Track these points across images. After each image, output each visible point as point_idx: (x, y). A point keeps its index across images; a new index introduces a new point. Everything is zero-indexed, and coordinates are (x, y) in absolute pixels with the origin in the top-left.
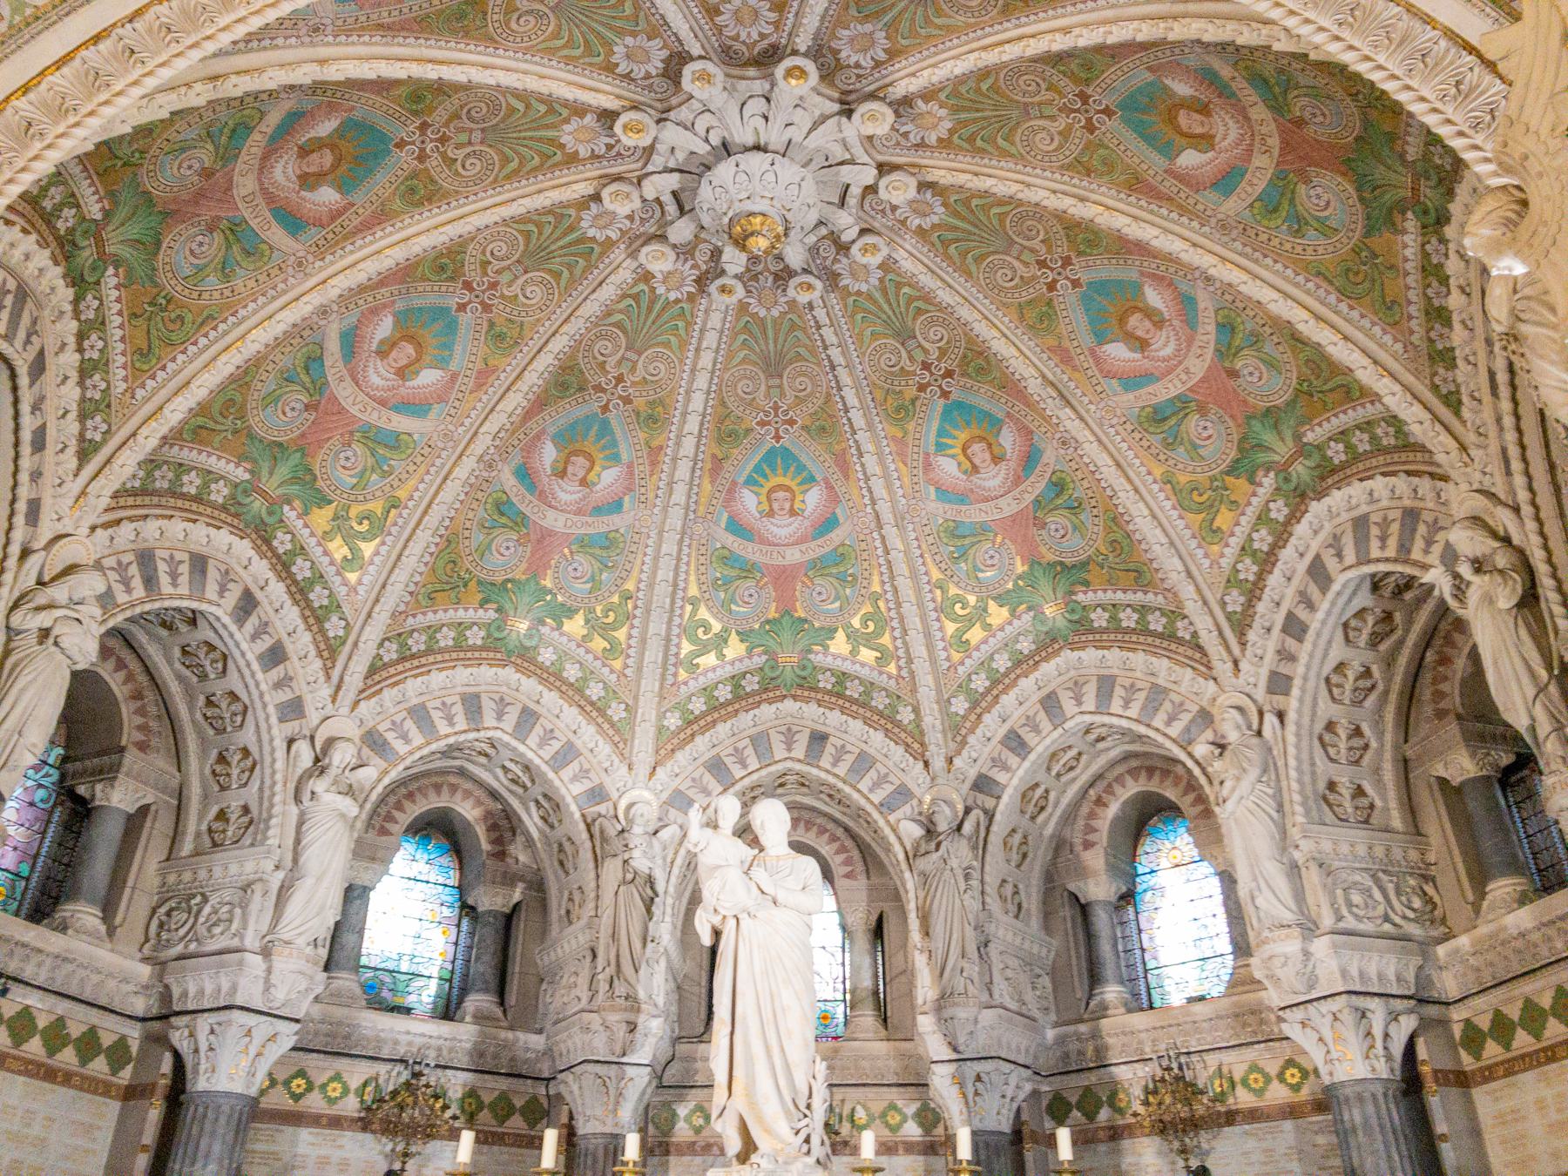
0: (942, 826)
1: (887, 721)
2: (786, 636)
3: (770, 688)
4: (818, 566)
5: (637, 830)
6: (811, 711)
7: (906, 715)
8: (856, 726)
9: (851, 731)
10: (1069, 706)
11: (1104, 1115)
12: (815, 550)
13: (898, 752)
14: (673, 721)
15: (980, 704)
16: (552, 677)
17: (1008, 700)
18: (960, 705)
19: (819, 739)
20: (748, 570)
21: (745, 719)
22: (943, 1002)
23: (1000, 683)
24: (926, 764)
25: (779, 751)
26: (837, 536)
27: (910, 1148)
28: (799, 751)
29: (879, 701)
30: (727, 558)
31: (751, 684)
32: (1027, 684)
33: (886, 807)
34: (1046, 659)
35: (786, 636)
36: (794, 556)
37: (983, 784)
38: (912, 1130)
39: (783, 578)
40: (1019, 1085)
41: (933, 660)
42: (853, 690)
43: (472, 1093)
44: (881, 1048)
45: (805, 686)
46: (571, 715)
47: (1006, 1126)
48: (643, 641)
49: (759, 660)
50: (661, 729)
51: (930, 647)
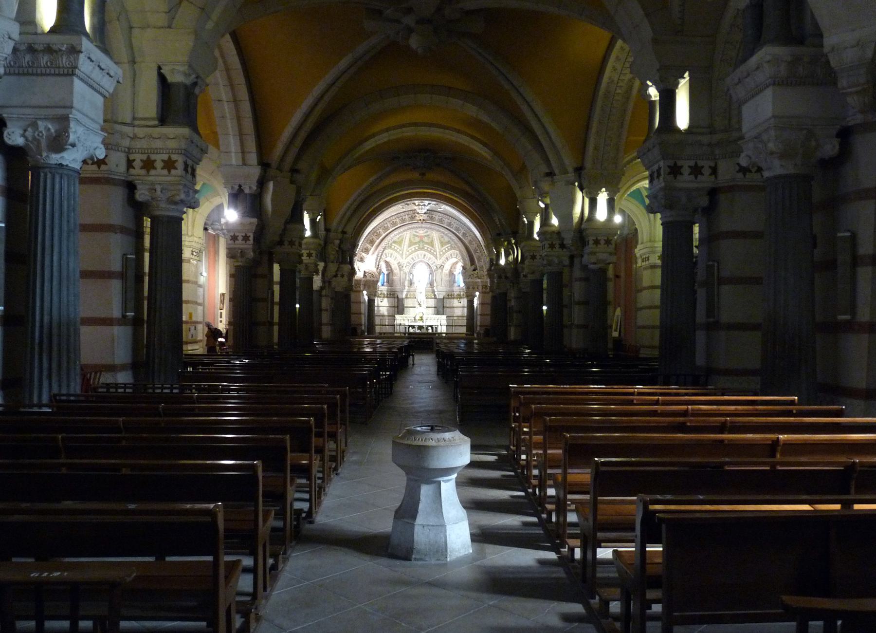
0: (438, 267)
1: (433, 254)
2: (421, 242)
3: (419, 249)
4: (426, 236)
5: (404, 267)
6: (424, 252)
7: (435, 253)
8: (429, 254)
9: (429, 255)
10: (453, 256)
11: (453, 297)
12: (425, 234)
13: (434, 258)
14: (408, 253)
15: (444, 254)
16: (394, 249)
17: (447, 254)
18: (441, 253)
19: (425, 255)
20: (417, 236)
21: (416, 253)
22: (437, 286)
23: (446, 252)
24: (437, 259)
25: (420, 257)
26: (428, 233)
27: (433, 298)
28: (422, 257)
29: (432, 251)
30: (414, 235)
31: (417, 248)
32: (449, 253)
33: (432, 264)
34: (451, 250)
35: (421, 242)
36: (423, 235)
37: (443, 263)
38: (433, 297)
39: (421, 237)
40: (444, 294)
41: (439, 248)
42: (429, 250)
43: (387, 294)
44: (430, 288)
45: (423, 249)
46: (396, 254)
47: (442, 297)
48: (404, 245)
49: (418, 245)
50: (406, 254)
51: (438, 246)
